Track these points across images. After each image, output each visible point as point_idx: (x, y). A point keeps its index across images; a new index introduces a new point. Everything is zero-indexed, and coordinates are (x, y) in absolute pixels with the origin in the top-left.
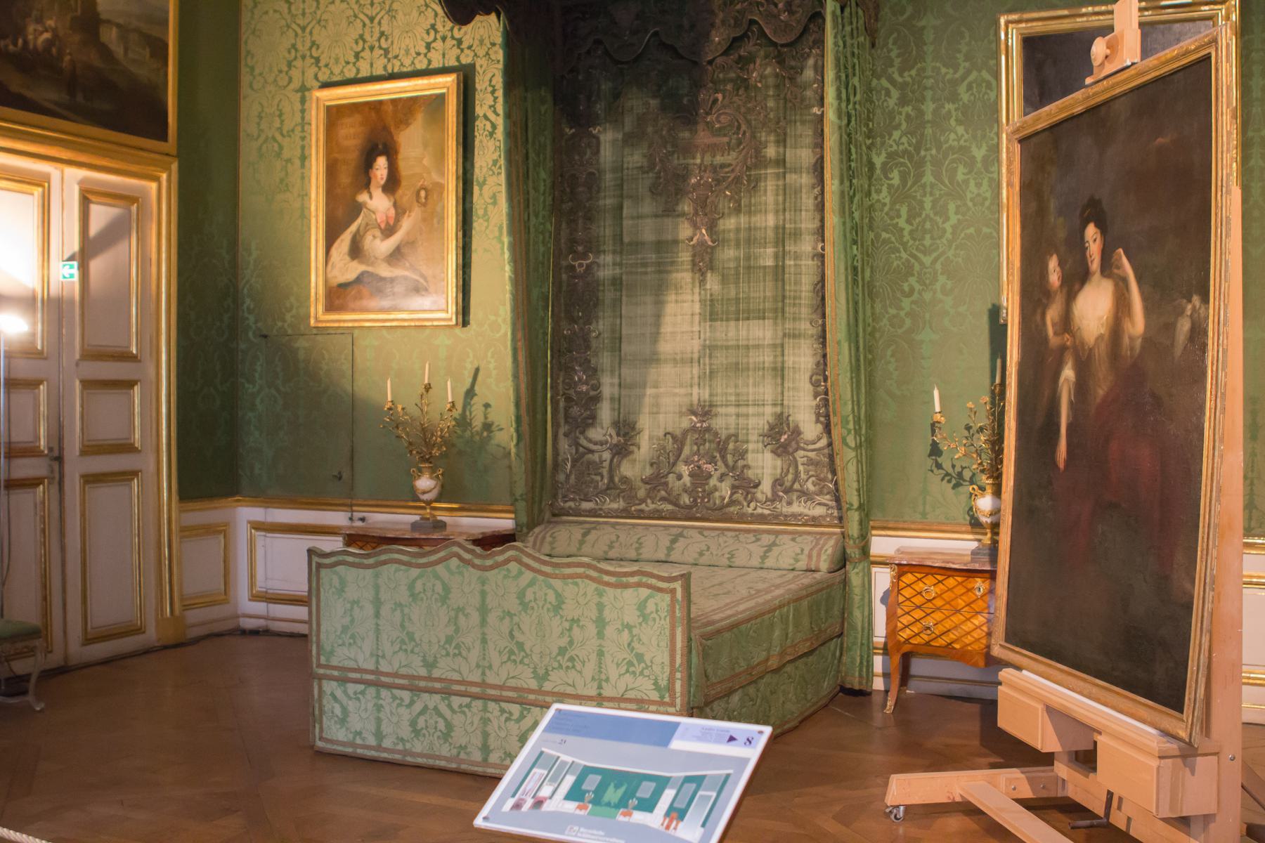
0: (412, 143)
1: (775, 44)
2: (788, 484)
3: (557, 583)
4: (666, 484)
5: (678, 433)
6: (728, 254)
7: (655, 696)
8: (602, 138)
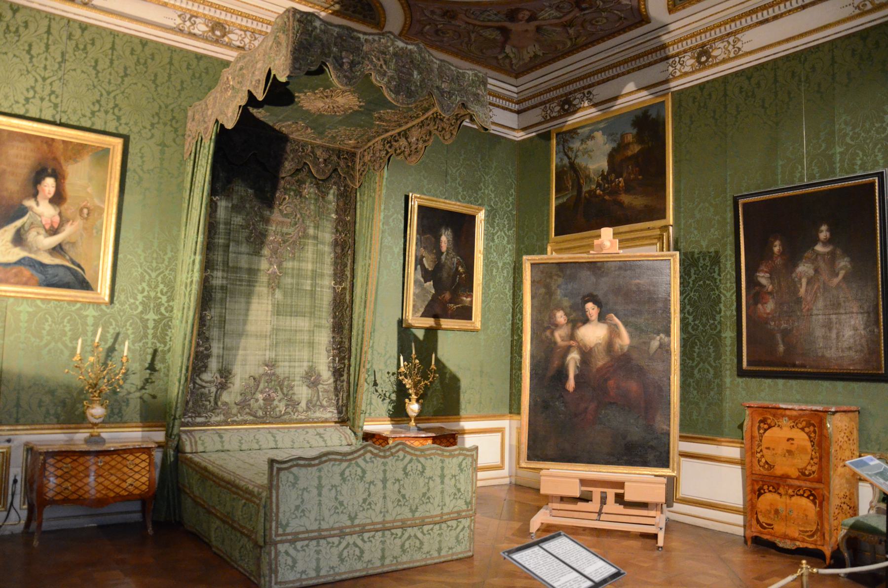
0: (77, 175)
1: (316, 178)
2: (314, 402)
3: (422, 460)
4: (249, 405)
5: (257, 376)
6: (288, 281)
7: (465, 507)
8: (219, 203)
